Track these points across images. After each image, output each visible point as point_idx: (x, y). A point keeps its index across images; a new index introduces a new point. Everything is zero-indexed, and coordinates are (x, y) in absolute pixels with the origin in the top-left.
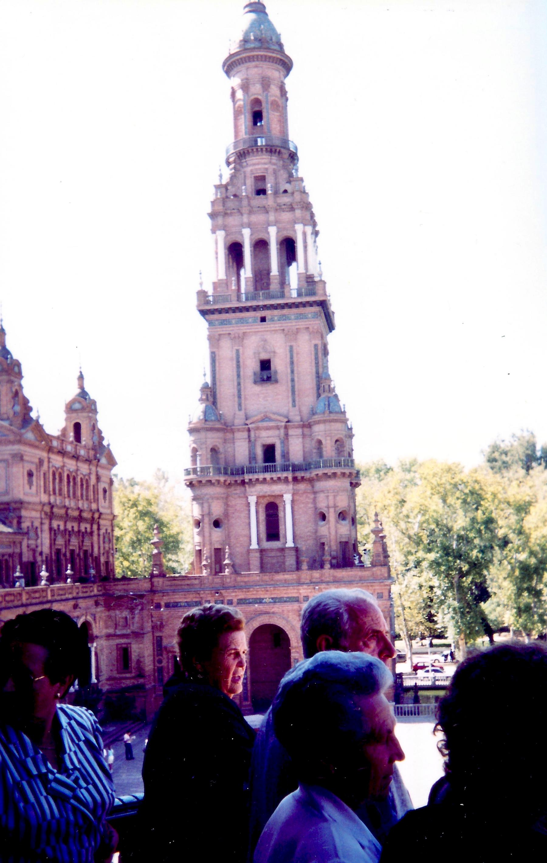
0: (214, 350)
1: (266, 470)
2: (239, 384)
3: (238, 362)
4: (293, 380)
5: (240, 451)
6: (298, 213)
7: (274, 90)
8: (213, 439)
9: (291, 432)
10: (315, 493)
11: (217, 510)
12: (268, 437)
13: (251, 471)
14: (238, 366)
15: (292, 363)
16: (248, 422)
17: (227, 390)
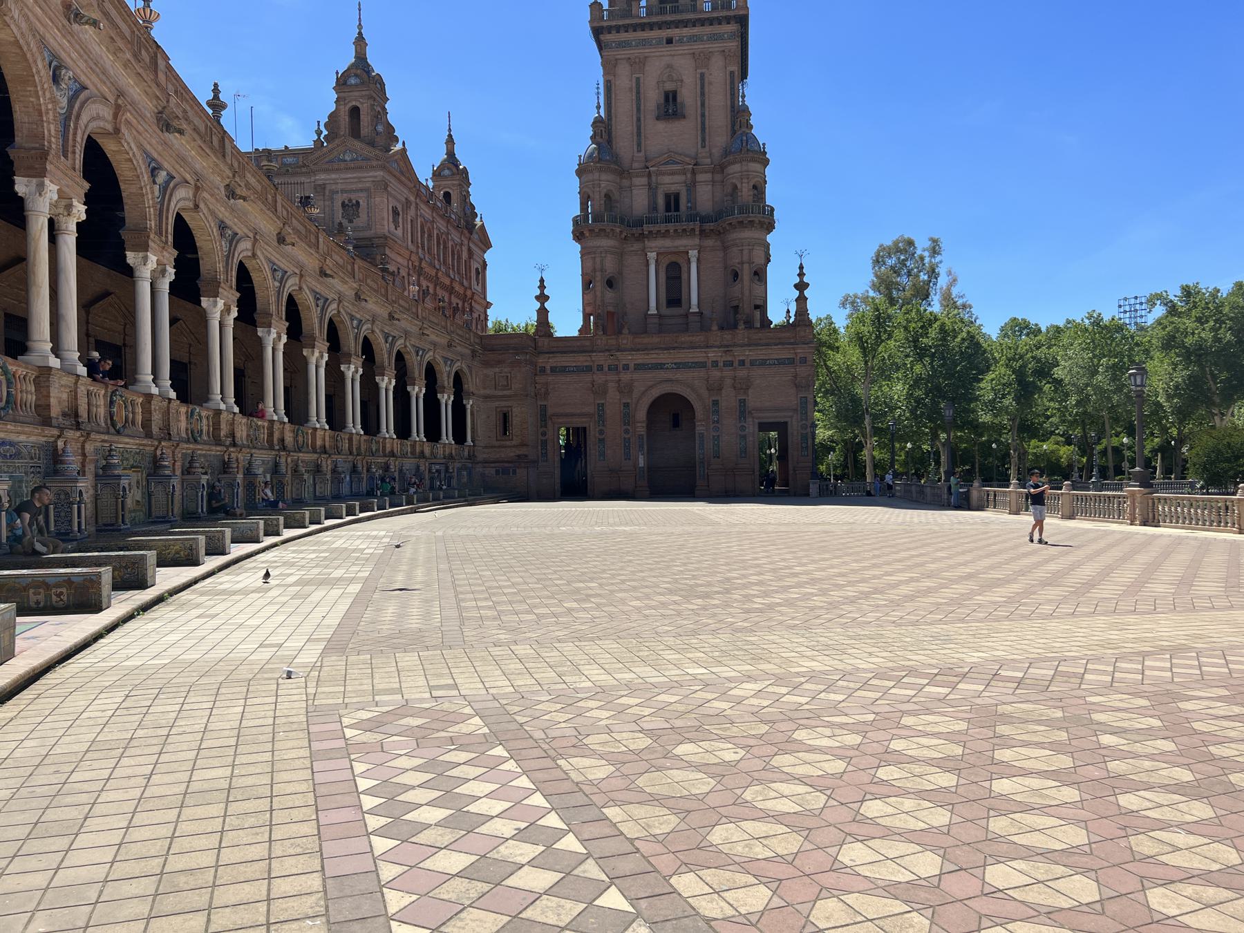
0: (611, 78)
1: (668, 220)
2: (639, 120)
3: (638, 93)
4: (703, 115)
5: (639, 201)
8: (606, 181)
9: (700, 177)
11: (610, 264)
12: (671, 182)
14: (638, 99)
15: (703, 94)
16: (649, 164)
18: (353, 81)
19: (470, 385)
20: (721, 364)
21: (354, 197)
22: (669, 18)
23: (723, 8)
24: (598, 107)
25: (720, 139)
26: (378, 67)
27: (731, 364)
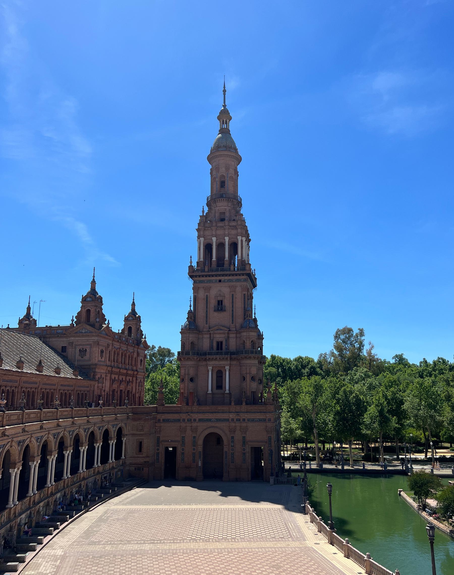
0: (196, 294)
1: (217, 354)
2: (207, 311)
3: (207, 301)
4: (233, 311)
5: (205, 344)
6: (239, 230)
7: (232, 171)
8: (192, 337)
9: (231, 336)
10: (241, 366)
11: (192, 372)
12: (219, 337)
13: (210, 354)
14: (207, 303)
15: (233, 302)
16: (210, 330)
17: (201, 314)
18: (89, 299)
19: (125, 432)
20: (235, 420)
21: (84, 347)
22: (219, 273)
23: (241, 270)
24: (190, 306)
25: (239, 320)
26: (100, 291)
27: (239, 420)
